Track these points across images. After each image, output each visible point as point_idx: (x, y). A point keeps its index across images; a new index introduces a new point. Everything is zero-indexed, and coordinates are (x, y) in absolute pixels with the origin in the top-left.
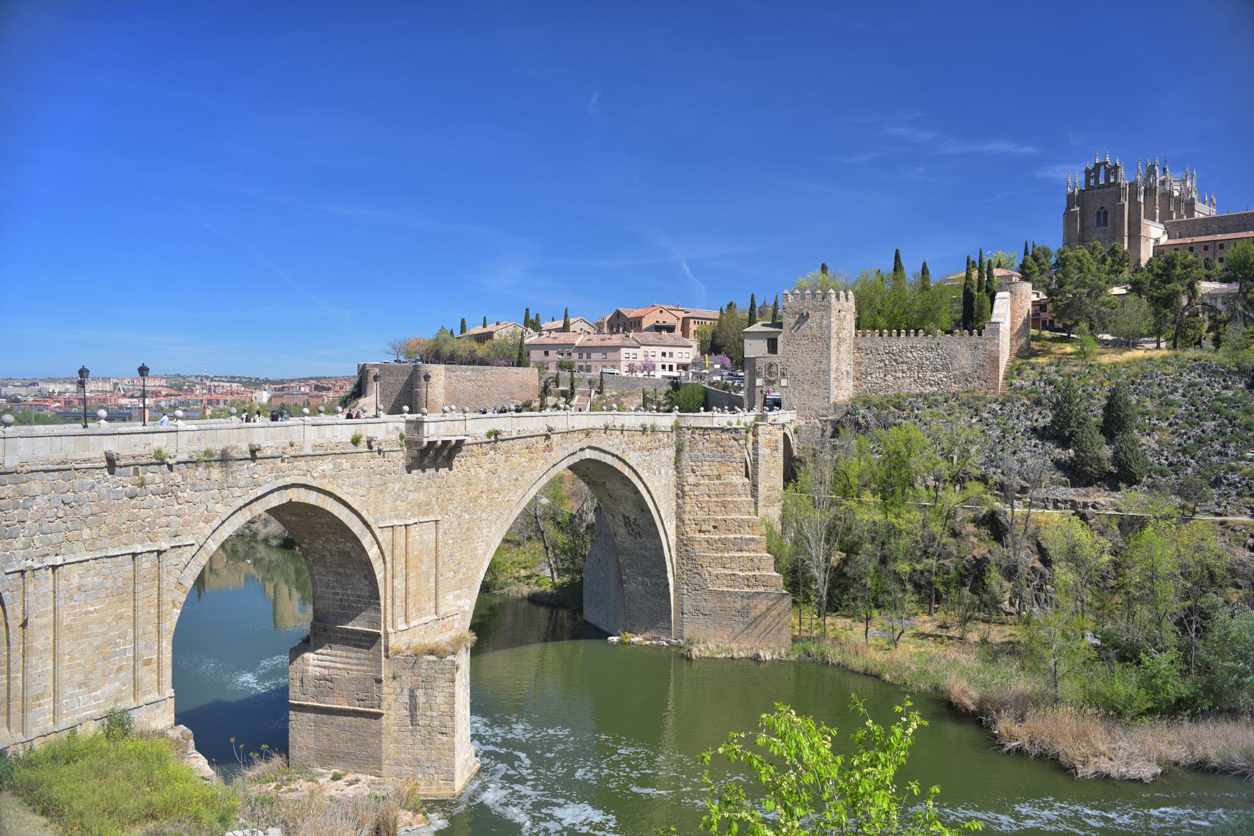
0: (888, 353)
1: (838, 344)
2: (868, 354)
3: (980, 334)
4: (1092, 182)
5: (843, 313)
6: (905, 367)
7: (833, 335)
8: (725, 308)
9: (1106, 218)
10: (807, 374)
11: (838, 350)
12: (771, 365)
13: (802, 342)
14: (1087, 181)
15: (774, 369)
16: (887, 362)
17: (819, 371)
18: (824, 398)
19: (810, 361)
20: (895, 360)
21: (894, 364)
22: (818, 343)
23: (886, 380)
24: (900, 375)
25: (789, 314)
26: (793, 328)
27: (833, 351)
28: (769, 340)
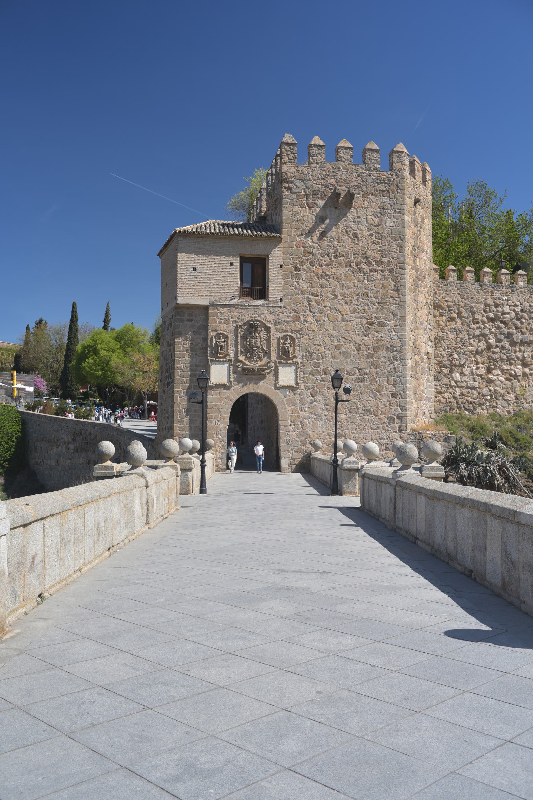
0: (492, 320)
1: (416, 285)
2: (452, 319)
7: (409, 259)
8: (32, 326)
15: (261, 335)
16: (492, 341)
17: (376, 349)
18: (391, 420)
19: (355, 321)
20: (509, 336)
22: (375, 275)
23: (490, 381)
24: (519, 369)
25: (297, 194)
26: (310, 233)
27: (409, 298)
28: (243, 260)
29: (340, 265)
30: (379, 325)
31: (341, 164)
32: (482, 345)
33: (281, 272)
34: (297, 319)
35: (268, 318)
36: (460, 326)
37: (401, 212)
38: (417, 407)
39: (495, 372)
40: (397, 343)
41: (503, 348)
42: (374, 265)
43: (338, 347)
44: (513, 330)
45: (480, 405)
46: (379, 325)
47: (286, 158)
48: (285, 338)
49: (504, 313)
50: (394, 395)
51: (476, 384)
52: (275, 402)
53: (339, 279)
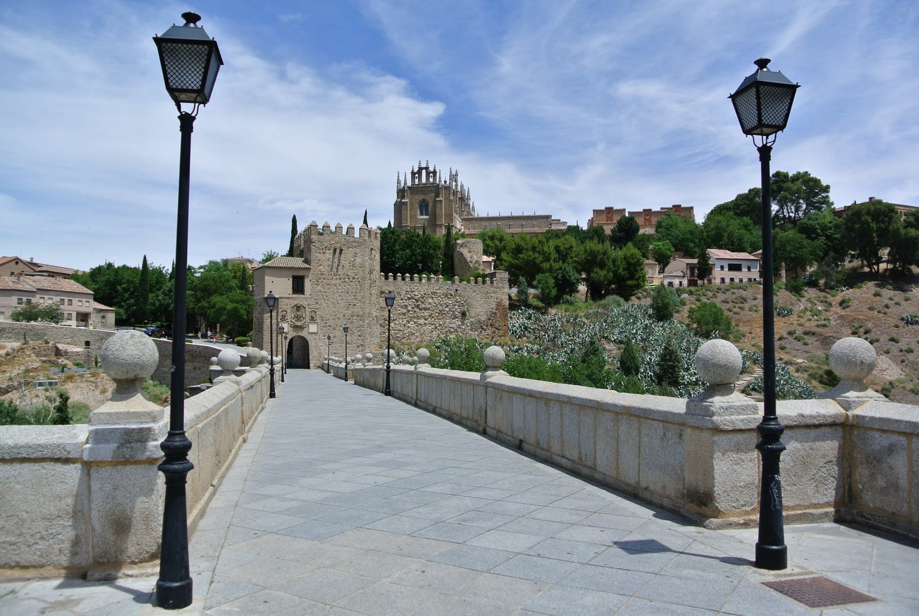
3: (492, 283)
4: (417, 181)
5: (373, 252)
6: (426, 314)
10: (339, 318)
12: (298, 308)
13: (334, 282)
19: (342, 304)
28: (294, 278)
29: (337, 279)
30: (353, 305)
33: (311, 283)
34: (317, 303)
35: (305, 303)
38: (370, 341)
39: (411, 323)
40: (361, 313)
41: (415, 311)
42: (351, 279)
43: (335, 315)
45: (404, 338)
46: (353, 305)
47: (313, 233)
48: (312, 312)
49: (415, 295)
50: (360, 336)
51: (401, 328)
52: (308, 339)
53: (336, 285)
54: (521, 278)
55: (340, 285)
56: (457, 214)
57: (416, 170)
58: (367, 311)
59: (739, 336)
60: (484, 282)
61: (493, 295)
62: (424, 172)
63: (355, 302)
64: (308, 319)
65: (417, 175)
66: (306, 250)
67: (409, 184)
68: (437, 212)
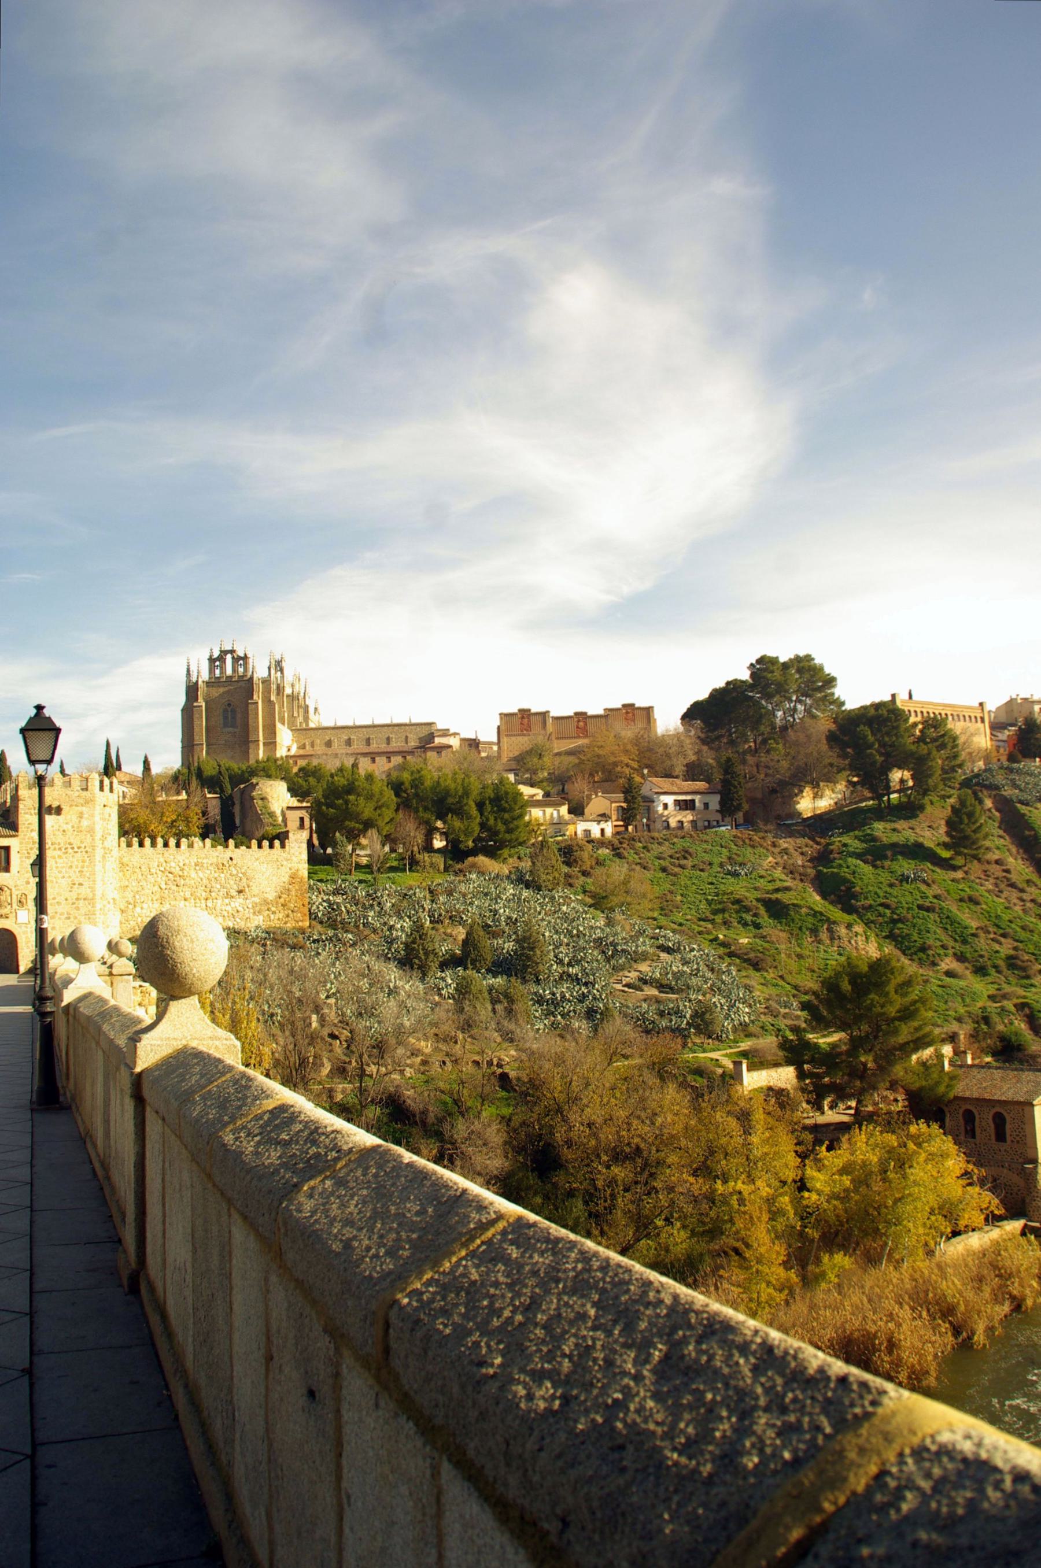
1: (104, 857)
4: (217, 672)
7: (98, 843)
9: (234, 718)
11: (104, 868)
14: (211, 671)
17: (77, 899)
21: (174, 888)
27: (98, 868)
31: (56, 788)
32: (156, 888)
33: (19, 855)
36: (140, 877)
37: (93, 816)
44: (178, 879)
52: (15, 932)
54: (337, 834)
55: (60, 857)
56: (283, 724)
57: (216, 654)
58: (98, 894)
59: (670, 907)
60: (271, 846)
61: (285, 863)
62: (229, 657)
63: (81, 880)
64: (15, 905)
65: (217, 663)
66: (12, 809)
67: (205, 676)
68: (251, 721)
